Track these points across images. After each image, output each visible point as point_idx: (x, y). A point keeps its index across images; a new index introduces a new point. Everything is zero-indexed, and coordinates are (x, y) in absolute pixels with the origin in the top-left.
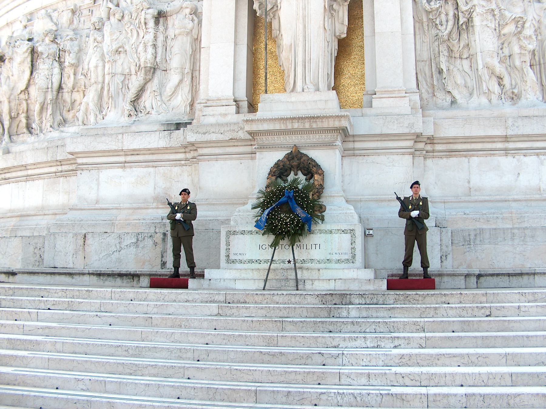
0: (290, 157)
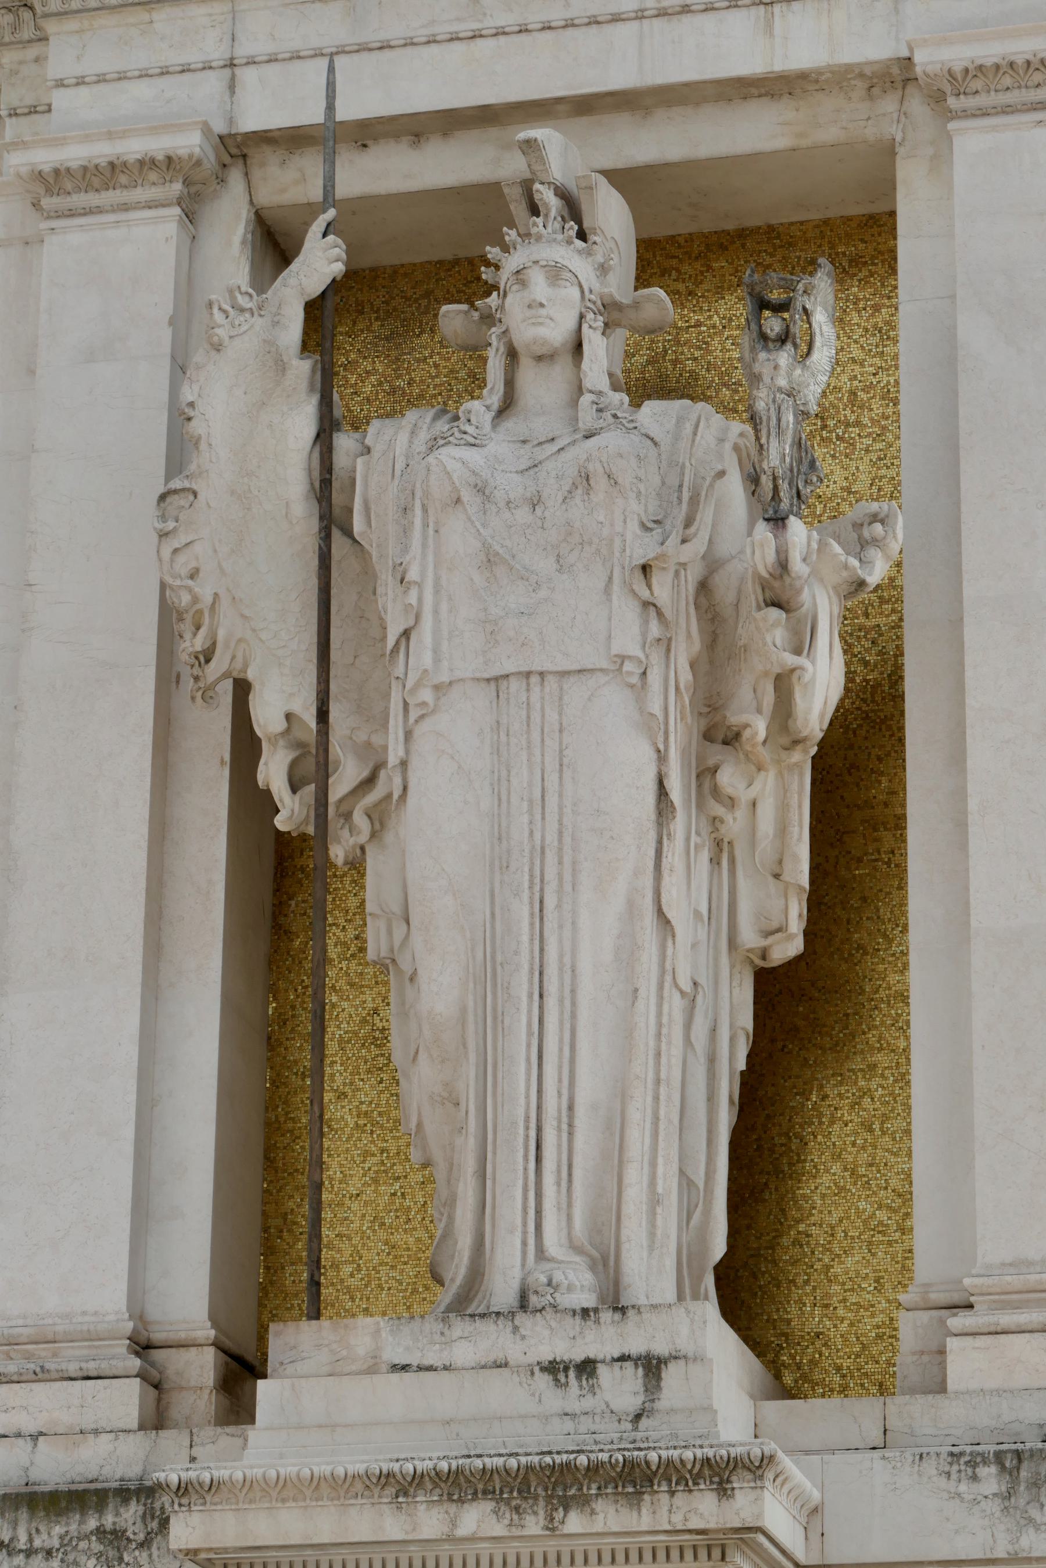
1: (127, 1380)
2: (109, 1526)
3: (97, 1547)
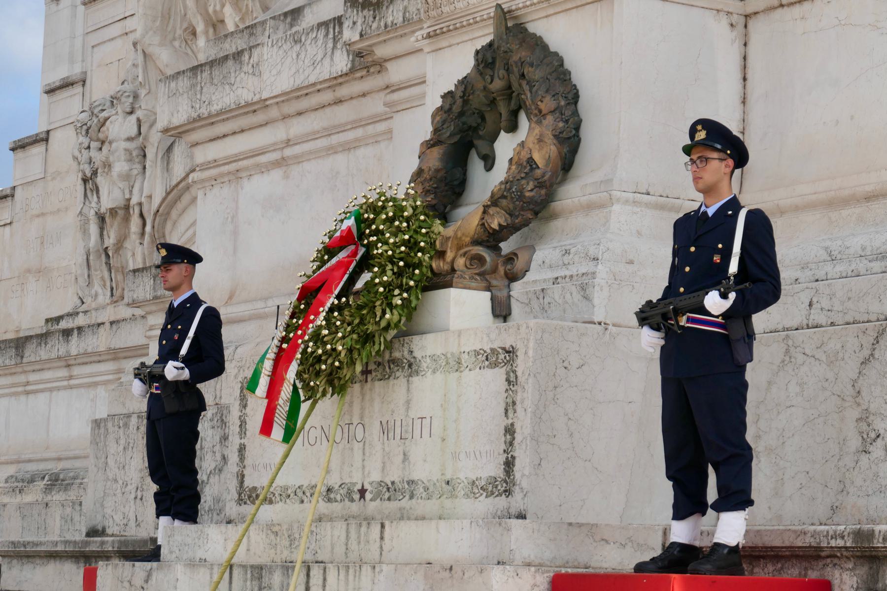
0: (486, 59)
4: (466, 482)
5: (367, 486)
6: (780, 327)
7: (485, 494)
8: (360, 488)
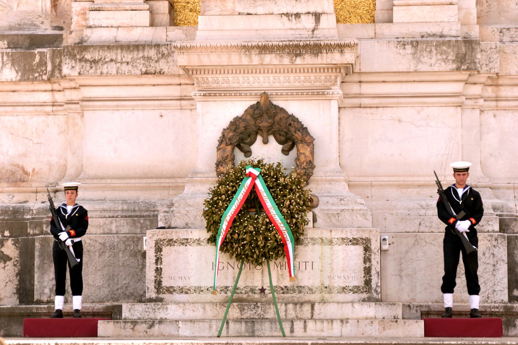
1: (145, 11)
2: (146, 56)
3: (142, 62)
4: (339, 288)
5: (265, 287)
6: (404, 231)
7: (352, 292)
8: (261, 288)
